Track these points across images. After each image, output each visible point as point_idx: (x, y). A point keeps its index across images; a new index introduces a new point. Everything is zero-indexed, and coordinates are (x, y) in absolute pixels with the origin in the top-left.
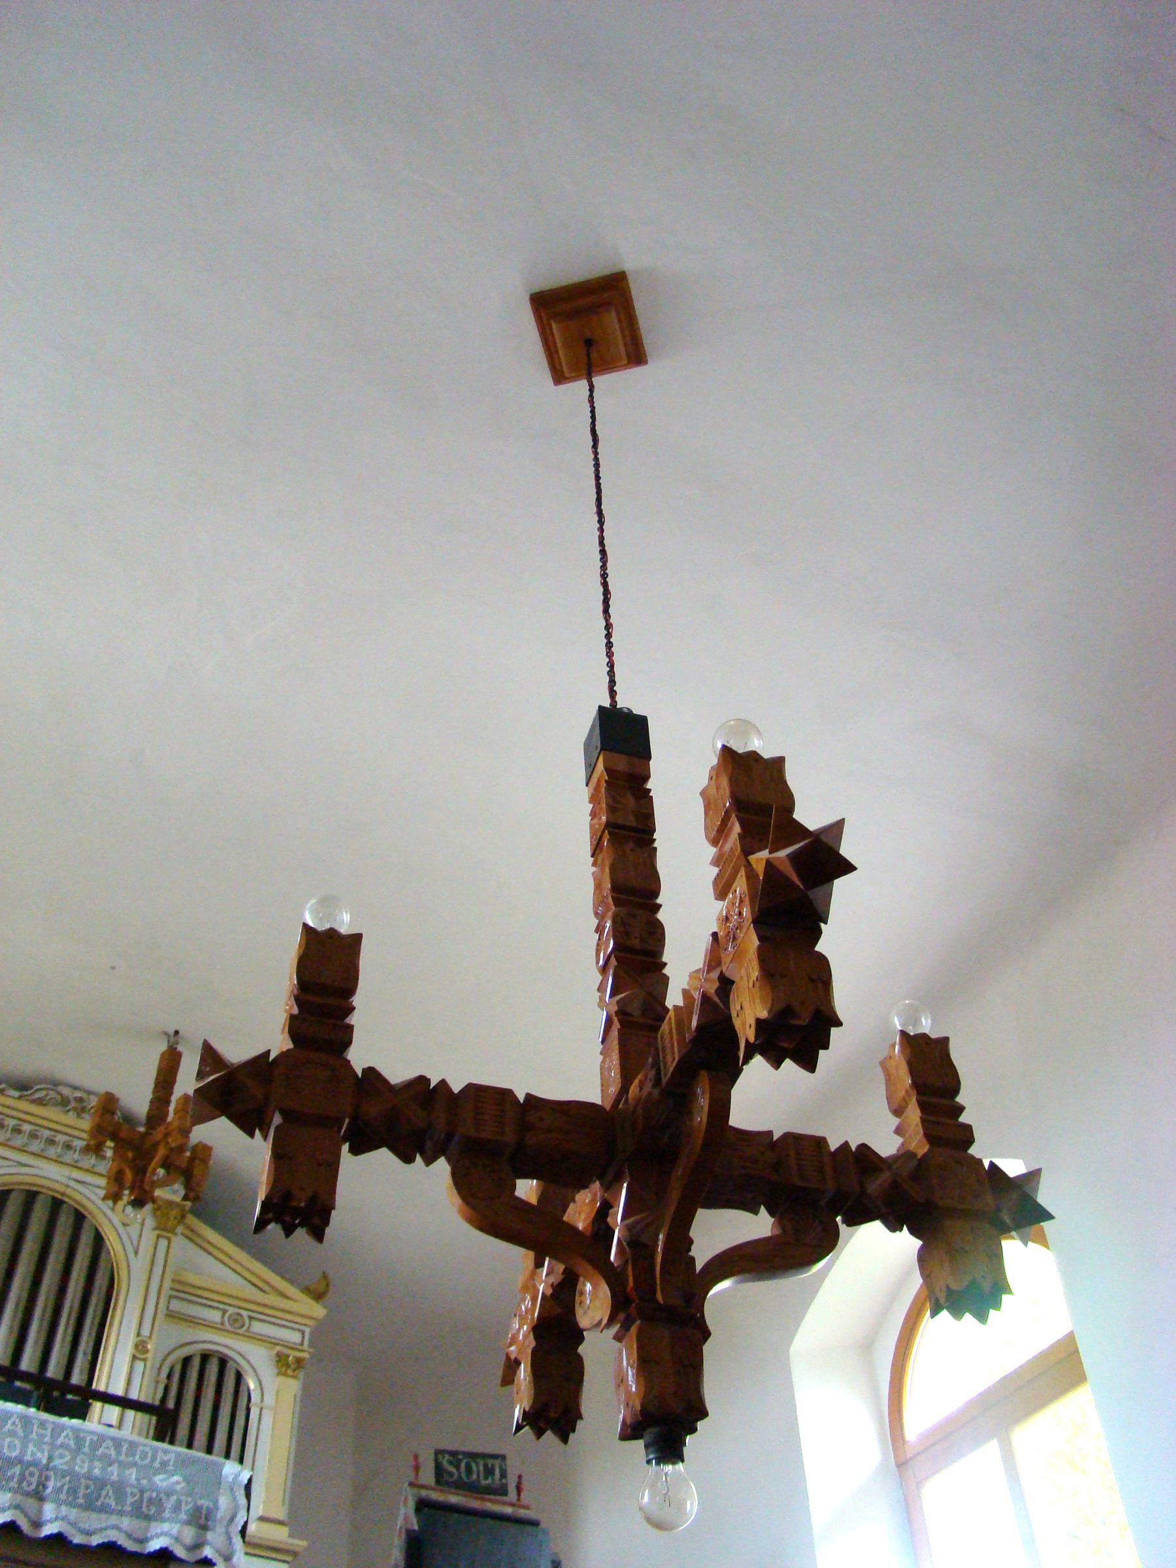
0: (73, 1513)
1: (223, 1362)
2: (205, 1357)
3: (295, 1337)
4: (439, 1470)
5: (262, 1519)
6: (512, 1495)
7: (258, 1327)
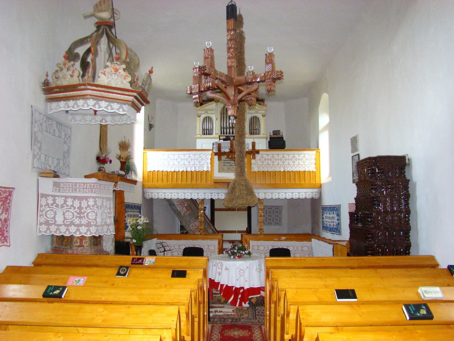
1: (256, 117)
2: (254, 117)
3: (264, 112)
4: (273, 133)
5: (263, 134)
6: (281, 134)
7: (259, 112)
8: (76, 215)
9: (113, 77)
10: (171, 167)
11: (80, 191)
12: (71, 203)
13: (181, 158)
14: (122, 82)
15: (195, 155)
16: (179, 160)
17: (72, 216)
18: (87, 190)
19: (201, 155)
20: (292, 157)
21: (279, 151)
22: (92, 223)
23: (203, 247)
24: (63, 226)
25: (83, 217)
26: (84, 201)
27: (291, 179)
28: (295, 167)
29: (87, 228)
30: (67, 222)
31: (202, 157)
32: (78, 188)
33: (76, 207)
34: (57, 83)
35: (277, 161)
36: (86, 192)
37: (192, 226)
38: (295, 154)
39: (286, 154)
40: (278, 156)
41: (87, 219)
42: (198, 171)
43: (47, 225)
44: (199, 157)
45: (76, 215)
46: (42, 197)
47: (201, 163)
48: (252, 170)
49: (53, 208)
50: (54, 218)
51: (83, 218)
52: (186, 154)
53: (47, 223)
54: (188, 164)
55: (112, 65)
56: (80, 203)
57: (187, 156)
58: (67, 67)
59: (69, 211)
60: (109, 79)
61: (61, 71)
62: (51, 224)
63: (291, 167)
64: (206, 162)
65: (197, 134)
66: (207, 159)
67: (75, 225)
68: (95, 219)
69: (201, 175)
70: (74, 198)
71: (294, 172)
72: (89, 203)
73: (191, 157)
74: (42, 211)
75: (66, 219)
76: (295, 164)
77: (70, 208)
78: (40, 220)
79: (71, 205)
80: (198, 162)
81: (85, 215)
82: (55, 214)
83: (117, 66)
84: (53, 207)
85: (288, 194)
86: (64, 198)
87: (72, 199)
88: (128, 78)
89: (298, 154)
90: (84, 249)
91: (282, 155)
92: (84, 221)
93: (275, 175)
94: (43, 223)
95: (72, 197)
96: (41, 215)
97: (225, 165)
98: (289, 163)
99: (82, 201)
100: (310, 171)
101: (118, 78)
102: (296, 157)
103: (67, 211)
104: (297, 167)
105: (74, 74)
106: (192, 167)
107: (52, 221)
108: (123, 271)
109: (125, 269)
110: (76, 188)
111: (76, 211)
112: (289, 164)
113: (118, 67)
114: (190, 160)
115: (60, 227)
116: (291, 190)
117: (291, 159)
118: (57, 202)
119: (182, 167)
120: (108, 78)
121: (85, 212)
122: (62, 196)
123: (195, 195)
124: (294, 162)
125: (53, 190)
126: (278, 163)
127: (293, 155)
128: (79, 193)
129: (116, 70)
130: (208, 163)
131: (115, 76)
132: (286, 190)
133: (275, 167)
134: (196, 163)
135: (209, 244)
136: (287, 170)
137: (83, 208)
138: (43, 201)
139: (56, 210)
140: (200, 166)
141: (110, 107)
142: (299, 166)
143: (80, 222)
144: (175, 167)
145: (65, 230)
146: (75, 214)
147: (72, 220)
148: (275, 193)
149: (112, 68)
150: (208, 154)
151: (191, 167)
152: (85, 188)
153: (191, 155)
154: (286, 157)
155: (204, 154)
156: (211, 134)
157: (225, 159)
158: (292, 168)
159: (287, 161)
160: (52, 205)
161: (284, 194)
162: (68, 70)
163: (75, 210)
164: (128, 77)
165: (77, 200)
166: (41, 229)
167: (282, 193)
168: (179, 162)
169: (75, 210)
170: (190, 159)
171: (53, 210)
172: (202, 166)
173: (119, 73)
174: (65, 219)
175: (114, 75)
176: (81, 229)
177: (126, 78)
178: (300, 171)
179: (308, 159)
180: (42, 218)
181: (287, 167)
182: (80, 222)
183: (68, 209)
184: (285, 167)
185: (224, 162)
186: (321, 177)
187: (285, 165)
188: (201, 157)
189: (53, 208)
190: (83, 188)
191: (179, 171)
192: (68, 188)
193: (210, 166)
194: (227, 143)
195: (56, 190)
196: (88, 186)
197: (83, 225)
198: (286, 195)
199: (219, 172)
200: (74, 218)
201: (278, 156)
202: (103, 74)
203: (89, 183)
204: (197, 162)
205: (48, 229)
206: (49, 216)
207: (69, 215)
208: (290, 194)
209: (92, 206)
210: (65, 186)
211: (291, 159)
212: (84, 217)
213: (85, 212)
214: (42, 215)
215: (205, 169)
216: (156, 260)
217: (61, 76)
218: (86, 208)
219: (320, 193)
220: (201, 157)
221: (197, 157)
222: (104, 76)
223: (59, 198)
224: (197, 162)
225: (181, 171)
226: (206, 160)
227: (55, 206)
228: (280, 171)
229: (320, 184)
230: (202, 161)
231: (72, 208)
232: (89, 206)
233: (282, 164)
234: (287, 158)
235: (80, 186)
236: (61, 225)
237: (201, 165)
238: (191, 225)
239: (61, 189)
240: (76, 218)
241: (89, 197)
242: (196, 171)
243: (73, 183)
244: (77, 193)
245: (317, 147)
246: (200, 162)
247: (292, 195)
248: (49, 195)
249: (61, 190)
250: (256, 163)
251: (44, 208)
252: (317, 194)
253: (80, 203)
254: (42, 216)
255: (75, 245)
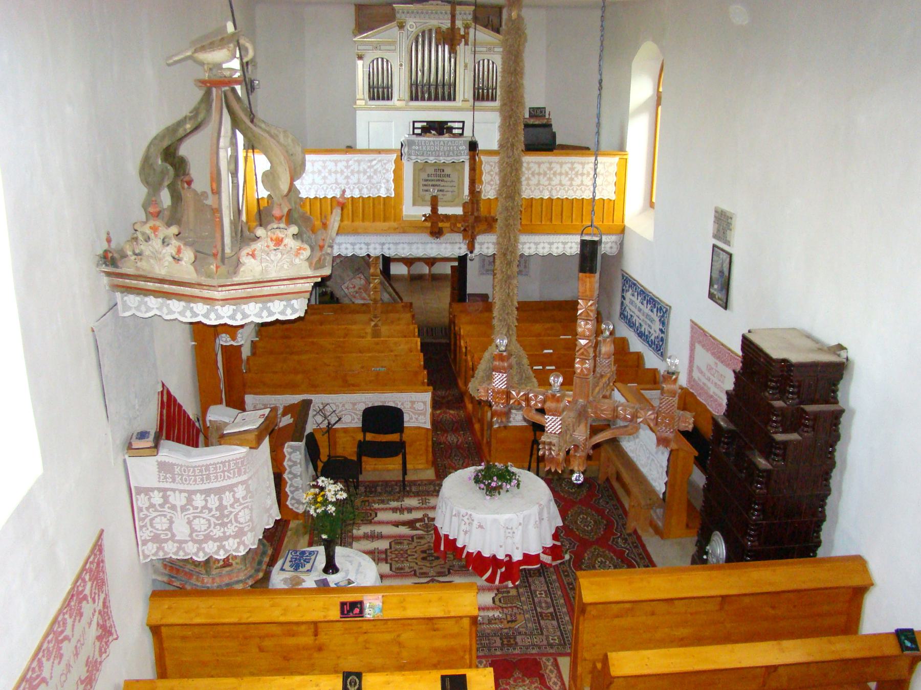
0: (445, 158)
6: (547, 116)
8: (214, 523)
9: (272, 257)
10: (307, 189)
11: (216, 477)
12: (203, 503)
13: (329, 168)
14: (292, 264)
15: (359, 162)
16: (325, 173)
17: (207, 525)
18: (230, 474)
19: (374, 162)
20: (568, 170)
21: (542, 155)
22: (246, 529)
23: (402, 404)
24: (190, 544)
25: (228, 523)
26: (227, 493)
27: (563, 215)
28: (573, 189)
29: (238, 540)
30: (197, 536)
31: (375, 167)
32: (212, 474)
33: (214, 507)
34: (139, 264)
35: (536, 177)
36: (228, 476)
37: (348, 288)
38: (575, 162)
39: (555, 162)
40: (539, 167)
41: (235, 524)
42: (367, 196)
43: (157, 543)
44: (370, 167)
45: (214, 523)
46: (138, 493)
47: (374, 181)
48: (483, 195)
49: (164, 511)
50: (170, 529)
51: (229, 525)
52: (341, 161)
53: (156, 539)
54: (345, 181)
55: (269, 233)
56: (221, 499)
57: (341, 166)
58: (161, 235)
59: (199, 517)
60: (264, 265)
61: (146, 241)
62: (166, 541)
63: (564, 189)
64: (384, 178)
65: (358, 97)
66: (387, 171)
67: (215, 540)
68: (251, 520)
69: (374, 204)
70: (207, 492)
71: (572, 202)
72: (237, 496)
73: (352, 168)
74: (143, 519)
75: (196, 531)
76: (574, 183)
77: (201, 512)
78: (141, 537)
79: (202, 507)
80: (366, 177)
81: (231, 520)
82: (171, 522)
83: (280, 232)
84: (164, 509)
85: (555, 245)
86: (186, 495)
87: (204, 496)
88: (304, 252)
89: (582, 163)
90: (232, 570)
91: (548, 165)
92: (231, 530)
93: (531, 206)
94: (149, 541)
95: (202, 492)
96: (141, 527)
97: (426, 191)
98: (561, 181)
99: (223, 495)
100: (604, 200)
101: (282, 257)
102: (576, 170)
103: (195, 518)
104: (577, 189)
105: (181, 255)
106: (354, 188)
107: (167, 535)
108: (353, 684)
109: (355, 681)
110: (207, 474)
111: (213, 516)
112: (561, 184)
113: (281, 235)
114: (349, 174)
115: (183, 545)
116: (562, 238)
117: (567, 174)
118: (171, 499)
119: (331, 188)
120: (261, 262)
121: (231, 512)
122: (181, 491)
123: (361, 249)
124: (572, 179)
125: (159, 478)
126: (539, 181)
127: (569, 165)
128: (216, 482)
129: (279, 242)
130: (388, 181)
131: (276, 255)
132: (552, 238)
133: (530, 189)
134: (362, 180)
135: (414, 399)
136: (555, 197)
137: (226, 508)
138: (141, 501)
139: (173, 515)
140: (371, 187)
141: (265, 311)
142: (581, 189)
143: (224, 533)
144: (316, 188)
145: (195, 550)
146: (213, 520)
147: (209, 530)
148: (530, 243)
149: (269, 239)
150: (389, 161)
151: (352, 188)
152: (226, 471)
153: (350, 162)
154: (557, 168)
155: (380, 161)
156: (388, 99)
157: (428, 178)
158: (567, 192)
159: (558, 177)
160: (162, 506)
161: (547, 246)
162: (166, 244)
163: (211, 514)
164: (304, 249)
165: (212, 496)
166: (147, 552)
167: (544, 243)
168: (325, 178)
169: (211, 514)
170: (349, 170)
171: (165, 516)
172: (376, 187)
173: (285, 245)
174: (193, 530)
175: (274, 252)
176: (227, 545)
177: (299, 253)
178: (583, 198)
179: (602, 174)
180: (144, 531)
181: (556, 189)
182: (224, 533)
183: (197, 513)
184: (552, 189)
185: (426, 183)
186: (626, 213)
187: (553, 186)
188: (373, 166)
189: (164, 511)
190: (223, 472)
191: (325, 198)
192: (193, 476)
193: (393, 187)
194: (432, 143)
195: (165, 478)
196: (232, 465)
197: (230, 536)
198: (550, 248)
199: (414, 204)
200: (212, 528)
201: (539, 167)
202: (250, 257)
203: (233, 460)
204: (363, 178)
205: (160, 548)
206: (158, 526)
207: (200, 524)
208: (561, 246)
209: (243, 498)
210: (185, 472)
211: (567, 174)
212: (231, 521)
213: (231, 512)
214: (145, 526)
215: (383, 194)
216: (383, 603)
217: (147, 253)
218: (232, 506)
219: (621, 245)
220: (373, 166)
221: (366, 167)
222: (252, 260)
223: (175, 493)
224: (363, 178)
225: (329, 196)
226: (384, 174)
227: (169, 508)
228: (542, 199)
229: (621, 228)
230: (375, 177)
231: (204, 511)
232: (237, 500)
233: (547, 183)
234: (558, 171)
235: (216, 468)
236: (186, 542)
237: (373, 184)
238: (346, 285)
239: (177, 476)
240: (214, 528)
241: (236, 485)
242: (363, 198)
243: (203, 466)
244: (212, 482)
245: (621, 148)
246: (370, 177)
247: (564, 248)
248: (152, 489)
249: (178, 479)
250: (492, 180)
251: (145, 512)
252: (614, 246)
253: (221, 499)
254: (144, 529)
255: (215, 567)
